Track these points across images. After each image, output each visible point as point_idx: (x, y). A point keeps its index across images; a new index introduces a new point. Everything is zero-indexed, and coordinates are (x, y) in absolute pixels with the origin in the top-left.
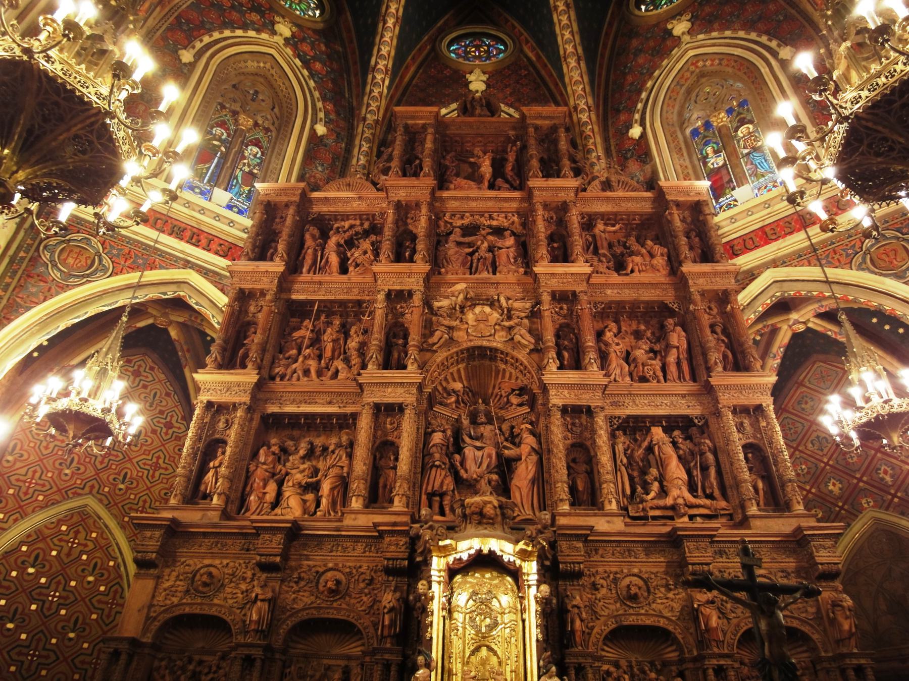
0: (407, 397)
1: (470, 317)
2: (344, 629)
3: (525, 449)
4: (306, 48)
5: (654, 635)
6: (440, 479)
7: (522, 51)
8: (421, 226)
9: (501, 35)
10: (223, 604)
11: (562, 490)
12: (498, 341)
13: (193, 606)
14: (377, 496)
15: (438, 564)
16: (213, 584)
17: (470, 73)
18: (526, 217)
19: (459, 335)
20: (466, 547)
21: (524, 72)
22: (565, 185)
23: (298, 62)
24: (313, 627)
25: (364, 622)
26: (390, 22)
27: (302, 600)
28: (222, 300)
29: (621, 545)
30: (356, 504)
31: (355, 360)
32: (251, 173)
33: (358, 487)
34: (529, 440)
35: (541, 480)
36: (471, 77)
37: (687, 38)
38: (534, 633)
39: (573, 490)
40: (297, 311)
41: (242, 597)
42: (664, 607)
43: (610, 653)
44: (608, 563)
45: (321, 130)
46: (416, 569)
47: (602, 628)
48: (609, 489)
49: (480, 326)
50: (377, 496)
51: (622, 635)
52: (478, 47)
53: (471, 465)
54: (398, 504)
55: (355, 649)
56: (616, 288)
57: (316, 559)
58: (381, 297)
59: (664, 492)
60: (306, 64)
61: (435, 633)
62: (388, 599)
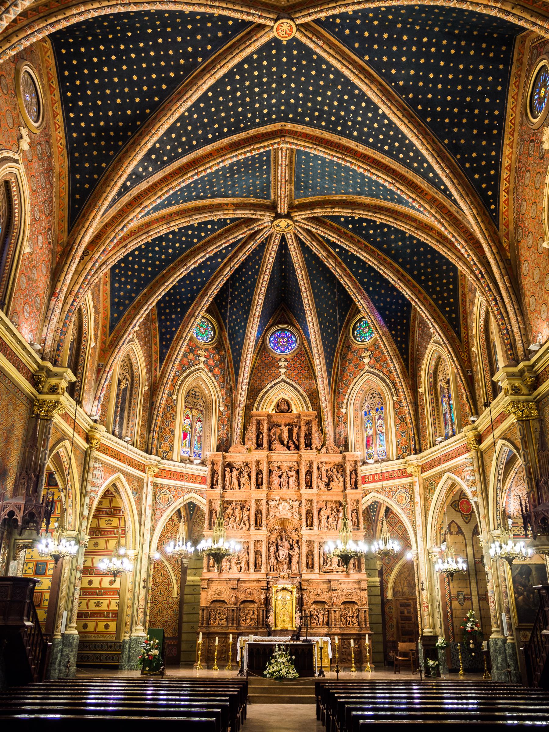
0: (264, 539)
1: (280, 507)
2: (253, 602)
3: (295, 553)
4: (211, 362)
5: (323, 603)
6: (273, 561)
7: (303, 343)
8: (264, 468)
9: (294, 331)
10: (224, 597)
11: (304, 566)
12: (289, 516)
13: (217, 598)
14: (257, 567)
15: (274, 590)
16: (220, 593)
17: (280, 360)
18: (299, 463)
19: (277, 514)
20: (280, 586)
21: (303, 359)
22: (314, 452)
23: (210, 374)
24: (244, 602)
25: (257, 601)
26: (248, 362)
27: (242, 596)
28: (205, 502)
29: (317, 582)
30: (252, 570)
31: (247, 523)
32: (200, 436)
33: (252, 565)
34: (297, 550)
35: (299, 562)
36: (280, 363)
37: (367, 367)
38: (295, 605)
39: (308, 564)
40: (226, 504)
41: (227, 595)
42: (325, 597)
43: (313, 606)
44: (314, 586)
45: (222, 409)
46: (267, 589)
47: (311, 601)
48: (316, 566)
49: (284, 511)
50: (257, 567)
51: (315, 602)
52: (283, 338)
53: (281, 555)
54: (263, 571)
55: (255, 606)
56: (327, 496)
57: (244, 586)
58: (253, 502)
59: (331, 565)
60: (211, 372)
61: (274, 605)
62: (263, 596)
